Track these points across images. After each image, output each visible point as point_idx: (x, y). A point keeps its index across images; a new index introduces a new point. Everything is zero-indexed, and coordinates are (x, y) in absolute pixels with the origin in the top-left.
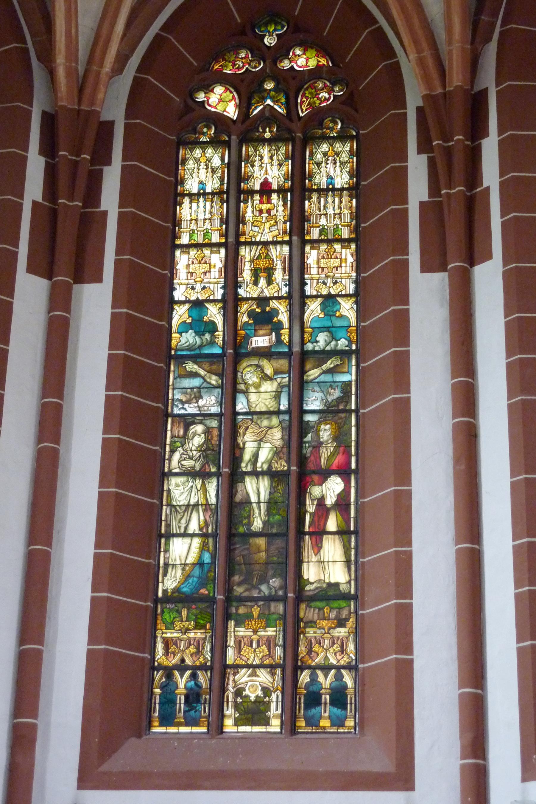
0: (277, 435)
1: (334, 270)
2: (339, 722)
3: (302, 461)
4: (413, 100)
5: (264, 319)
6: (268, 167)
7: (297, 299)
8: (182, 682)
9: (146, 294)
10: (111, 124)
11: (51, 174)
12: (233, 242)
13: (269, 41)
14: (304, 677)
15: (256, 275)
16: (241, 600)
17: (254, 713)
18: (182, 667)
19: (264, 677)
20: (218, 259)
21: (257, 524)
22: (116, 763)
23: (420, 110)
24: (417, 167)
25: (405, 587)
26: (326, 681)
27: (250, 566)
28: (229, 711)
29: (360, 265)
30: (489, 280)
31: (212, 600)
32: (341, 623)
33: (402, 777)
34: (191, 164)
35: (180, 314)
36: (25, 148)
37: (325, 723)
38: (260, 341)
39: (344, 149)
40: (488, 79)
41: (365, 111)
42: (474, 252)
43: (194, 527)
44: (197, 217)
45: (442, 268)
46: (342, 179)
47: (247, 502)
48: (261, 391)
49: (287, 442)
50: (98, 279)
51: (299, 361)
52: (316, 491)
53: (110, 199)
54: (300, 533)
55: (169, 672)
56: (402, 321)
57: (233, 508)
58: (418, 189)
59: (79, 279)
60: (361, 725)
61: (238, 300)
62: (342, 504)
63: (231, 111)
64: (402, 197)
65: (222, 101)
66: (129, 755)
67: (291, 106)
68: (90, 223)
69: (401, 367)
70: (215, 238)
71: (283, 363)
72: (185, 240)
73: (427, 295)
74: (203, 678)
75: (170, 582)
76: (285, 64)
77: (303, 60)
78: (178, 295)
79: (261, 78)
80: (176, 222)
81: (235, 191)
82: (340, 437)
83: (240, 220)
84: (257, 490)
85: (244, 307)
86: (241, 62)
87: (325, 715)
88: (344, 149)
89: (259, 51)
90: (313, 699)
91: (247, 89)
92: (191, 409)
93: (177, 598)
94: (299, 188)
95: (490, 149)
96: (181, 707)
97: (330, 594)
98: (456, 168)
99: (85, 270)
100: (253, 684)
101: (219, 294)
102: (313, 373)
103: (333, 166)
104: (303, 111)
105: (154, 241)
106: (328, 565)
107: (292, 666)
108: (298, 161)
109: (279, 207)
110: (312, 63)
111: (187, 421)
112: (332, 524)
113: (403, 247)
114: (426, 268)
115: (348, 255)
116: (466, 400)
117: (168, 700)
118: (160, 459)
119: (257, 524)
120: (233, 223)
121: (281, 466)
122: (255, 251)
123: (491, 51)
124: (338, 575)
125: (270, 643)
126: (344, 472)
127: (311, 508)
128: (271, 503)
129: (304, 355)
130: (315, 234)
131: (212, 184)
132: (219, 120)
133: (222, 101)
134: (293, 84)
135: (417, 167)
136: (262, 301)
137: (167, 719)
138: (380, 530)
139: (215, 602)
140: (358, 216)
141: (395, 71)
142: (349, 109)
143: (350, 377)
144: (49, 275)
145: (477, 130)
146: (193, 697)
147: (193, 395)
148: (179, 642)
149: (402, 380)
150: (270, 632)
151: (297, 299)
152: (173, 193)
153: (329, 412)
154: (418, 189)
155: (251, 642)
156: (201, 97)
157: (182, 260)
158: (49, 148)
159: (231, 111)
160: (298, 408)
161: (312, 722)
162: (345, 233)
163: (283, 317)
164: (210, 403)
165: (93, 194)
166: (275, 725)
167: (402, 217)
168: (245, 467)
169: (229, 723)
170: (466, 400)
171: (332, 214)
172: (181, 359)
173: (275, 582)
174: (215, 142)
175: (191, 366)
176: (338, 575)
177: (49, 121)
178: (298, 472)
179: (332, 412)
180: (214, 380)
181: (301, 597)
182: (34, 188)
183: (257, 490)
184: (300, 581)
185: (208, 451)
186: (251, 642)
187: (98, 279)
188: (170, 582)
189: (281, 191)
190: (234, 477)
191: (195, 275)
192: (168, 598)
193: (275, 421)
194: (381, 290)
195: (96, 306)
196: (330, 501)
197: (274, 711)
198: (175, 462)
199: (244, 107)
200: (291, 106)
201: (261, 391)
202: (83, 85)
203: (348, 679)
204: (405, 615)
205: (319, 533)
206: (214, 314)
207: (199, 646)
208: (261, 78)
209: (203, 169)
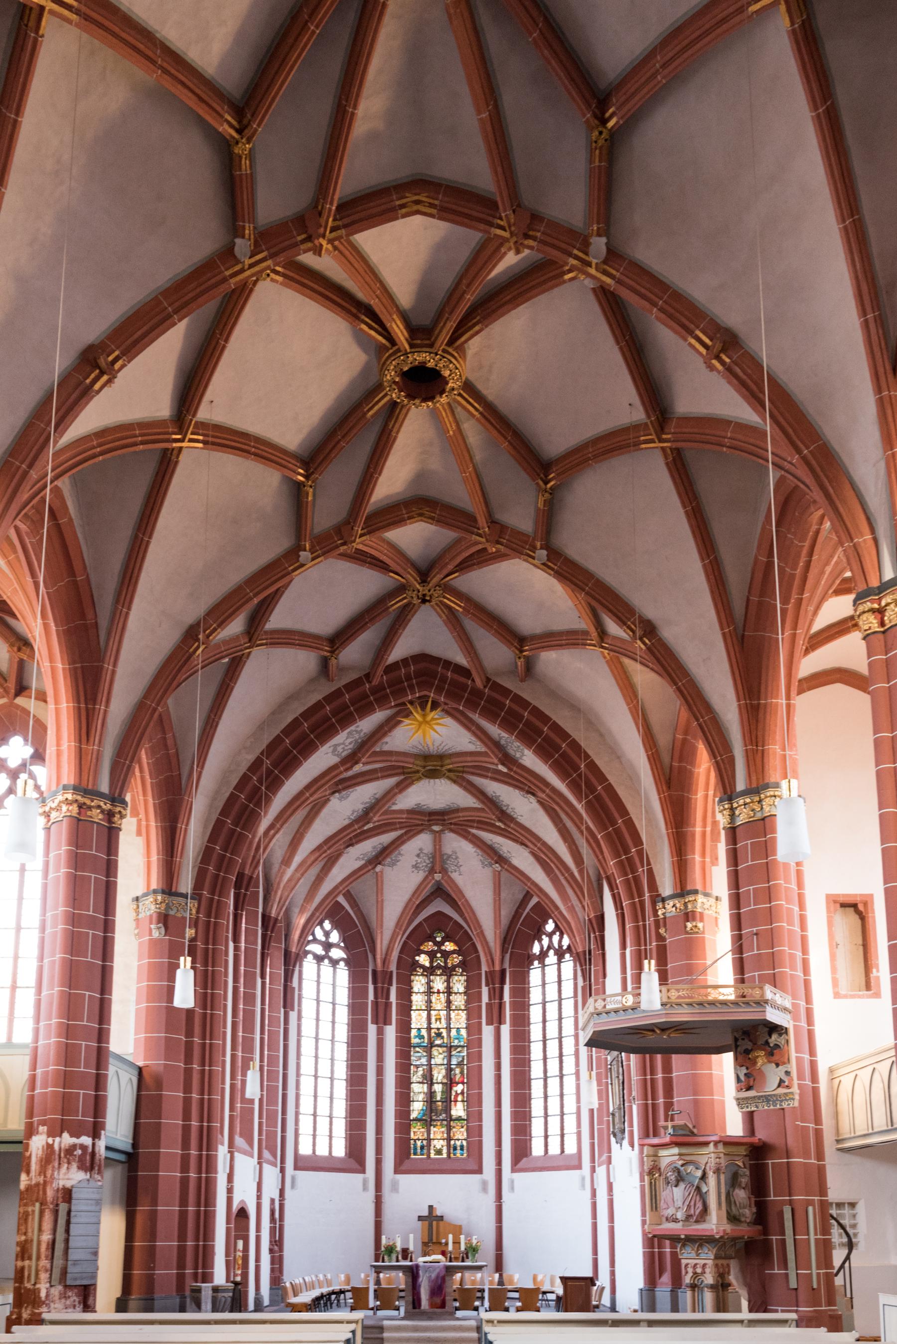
0: (443, 1072)
1: (460, 1019)
2: (462, 1155)
3: (451, 1080)
4: (484, 968)
5: (439, 1035)
6: (439, 983)
7: (449, 1029)
8: (419, 1143)
9: (405, 1027)
10: (391, 972)
11: (376, 989)
12: (429, 1009)
13: (438, 939)
14: (452, 1142)
15: (436, 1020)
16: (435, 1120)
17: (439, 1152)
18: (419, 1139)
19: (441, 1142)
21: (439, 1098)
22: (403, 1168)
23: (486, 972)
24: (485, 991)
25: (480, 1120)
26: (458, 1143)
27: (438, 1110)
28: (432, 1152)
29: (468, 1019)
30: (506, 1029)
31: (426, 1120)
32: (462, 1127)
33: (479, 1171)
34: (415, 982)
35: (414, 1033)
36: (367, 983)
37: (458, 1155)
38: (438, 1042)
39: (463, 978)
40: (506, 965)
41: (469, 965)
42: (501, 1021)
43: (421, 1099)
44: (418, 1000)
45: (492, 1024)
46: (462, 990)
47: (435, 1092)
48: (439, 1057)
49: (447, 1074)
50: (390, 1024)
51: (450, 1048)
52: (455, 1089)
53: (393, 998)
54: (451, 1101)
55: (415, 1140)
56: (480, 1040)
57: (431, 1094)
59: (385, 1024)
60: (468, 1155)
61: (431, 1029)
62: (462, 1093)
63: (427, 964)
64: (480, 1000)
65: (423, 960)
66: (406, 1165)
67: (446, 963)
68: (388, 1005)
69: (480, 1054)
70: (424, 1008)
71: (445, 1049)
72: (414, 1008)
73: (488, 1032)
74: (425, 1142)
76: (443, 948)
78: (412, 1026)
79: (437, 952)
80: (411, 1002)
81: (429, 991)
82: (462, 1073)
83: (431, 1002)
84: (438, 1088)
85: (433, 1031)
86: (429, 946)
87: (458, 1152)
88: (463, 978)
89: (436, 943)
90: (455, 1149)
91: (432, 955)
92: (418, 1063)
93: (416, 1119)
94: (449, 991)
96: (419, 1151)
97: (459, 1119)
99: (387, 1022)
100: (439, 1144)
101: (425, 1026)
102: (454, 1053)
103: (459, 984)
104: (450, 965)
105: (406, 1008)
106: (458, 1110)
107: (449, 1139)
108: (448, 981)
109: (443, 997)
110: (452, 948)
111: (417, 1067)
112: (460, 1098)
113: (480, 1017)
114: (487, 1024)
116: (498, 1066)
117: (415, 1149)
118: (409, 1078)
119: (439, 1098)
120: (429, 1002)
121: (445, 1081)
122: (436, 1012)
123: (508, 956)
125: (443, 1132)
126: (463, 1083)
127: (454, 1093)
128: (442, 1092)
129: (451, 1047)
130: (454, 1007)
131: (422, 989)
132: (422, 967)
133: (423, 960)
134: (446, 955)
135: (485, 991)
136: (438, 1029)
137: (415, 1154)
138: (474, 1101)
139: (427, 1121)
140: (467, 1002)
141: (478, 957)
142: (463, 965)
143: (465, 1054)
144: (377, 1024)
145: (503, 982)
146: (422, 1148)
147: (418, 1058)
148: (417, 1132)
149: (480, 1058)
150: (443, 1129)
151: (449, 1029)
156: (417, 958)
158: (375, 982)
159: (427, 964)
160: (449, 1064)
161: (454, 1154)
162: (463, 1007)
163: (445, 1034)
164: (424, 1061)
165: (388, 997)
166: (445, 1156)
167: (480, 1007)
168: (434, 1081)
169: (432, 1156)
171: (459, 1001)
172: (415, 1047)
173: (444, 1115)
174: (422, 975)
175: (417, 1049)
177: (374, 972)
178: (450, 1083)
179: (460, 1064)
180: (425, 1054)
181: (451, 1120)
182: (371, 997)
183: (438, 1088)
184: (451, 1116)
185: (424, 1076)
186: (438, 1132)
187: (390, 1024)
188: (414, 1115)
189: (443, 993)
190: (431, 1084)
191: (418, 1020)
192: (414, 1120)
193: (443, 1067)
194: (474, 1029)
195: (391, 1032)
196: (459, 1092)
197: (445, 1151)
198: (414, 1079)
199: (431, 962)
200: (446, 963)
201: (439, 1057)
202: (385, 961)
203: (465, 1143)
204: (480, 1127)
205: (456, 1101)
206: (424, 1032)
207: (423, 1133)
208: (437, 952)
209: (419, 983)
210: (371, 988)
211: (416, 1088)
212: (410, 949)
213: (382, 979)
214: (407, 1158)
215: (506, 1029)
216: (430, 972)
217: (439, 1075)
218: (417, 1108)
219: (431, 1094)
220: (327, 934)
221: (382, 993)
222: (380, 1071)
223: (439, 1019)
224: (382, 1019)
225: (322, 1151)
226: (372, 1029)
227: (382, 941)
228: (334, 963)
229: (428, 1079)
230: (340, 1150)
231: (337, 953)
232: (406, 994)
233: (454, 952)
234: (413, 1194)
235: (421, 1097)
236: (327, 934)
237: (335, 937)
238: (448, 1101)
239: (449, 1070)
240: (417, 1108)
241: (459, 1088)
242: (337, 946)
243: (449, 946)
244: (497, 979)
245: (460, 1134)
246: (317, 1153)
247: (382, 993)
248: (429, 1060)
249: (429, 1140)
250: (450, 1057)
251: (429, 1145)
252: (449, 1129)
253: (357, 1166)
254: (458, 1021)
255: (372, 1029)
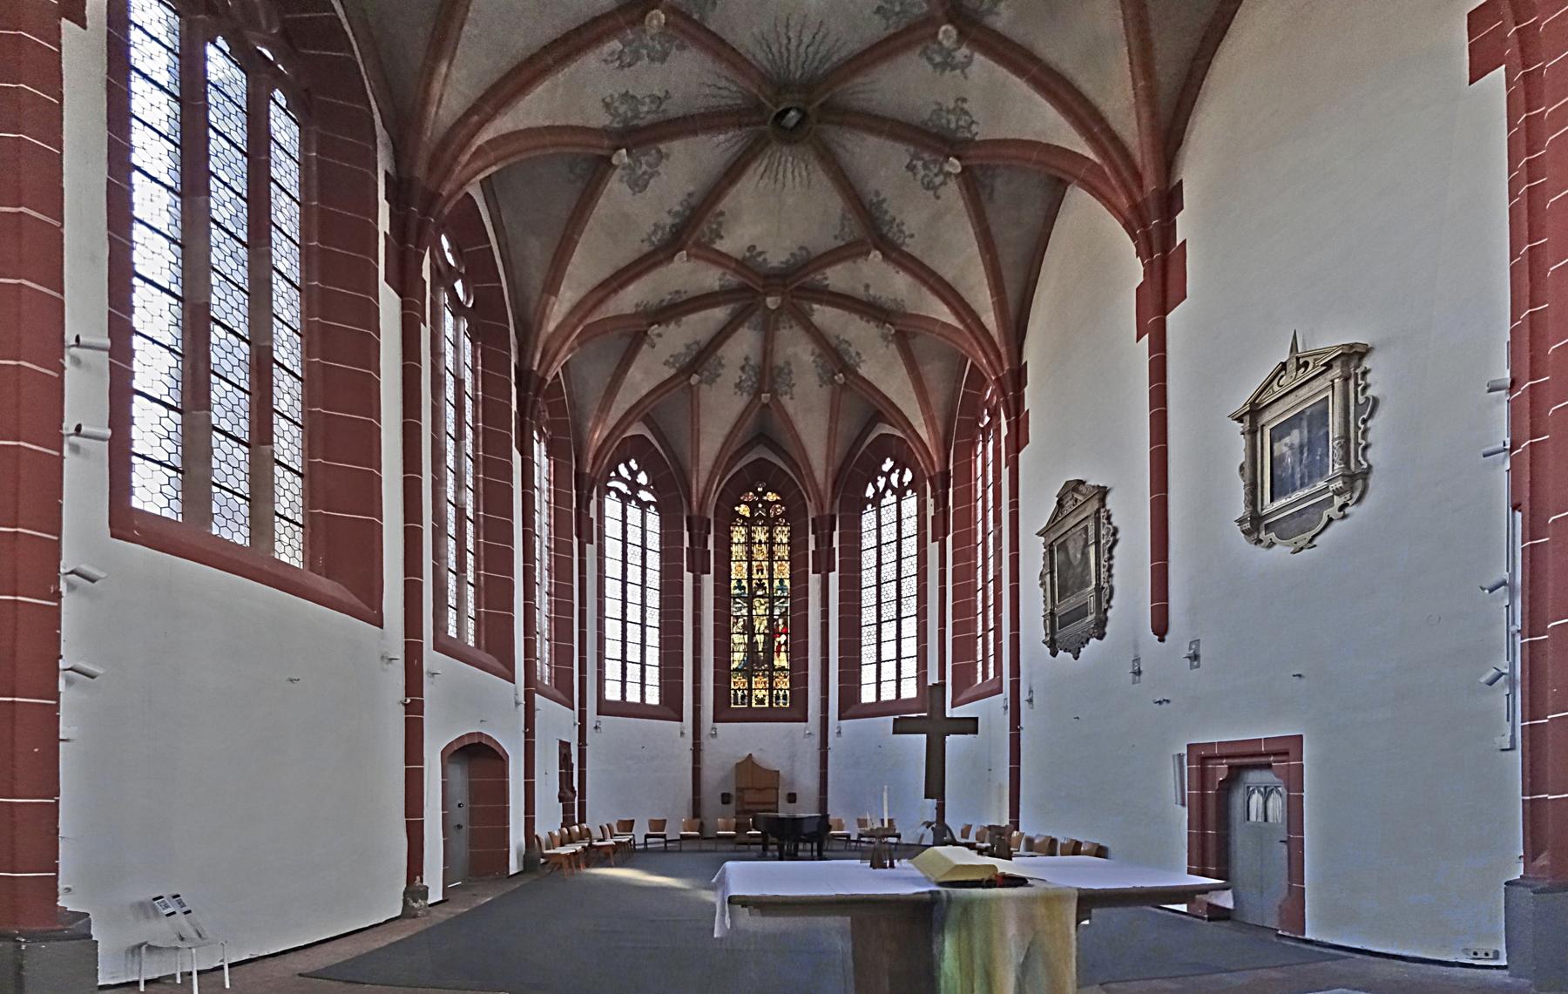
1: (783, 571)
5: (761, 586)
6: (761, 535)
7: (771, 580)
9: (723, 577)
12: (750, 560)
17: (761, 701)
20: (745, 565)
24: (811, 538)
27: (758, 662)
29: (791, 569)
30: (834, 577)
35: (734, 583)
44: (737, 551)
46: (785, 540)
48: (760, 609)
51: (772, 599)
53: (711, 546)
58: (812, 547)
65: (743, 510)
67: (768, 513)
73: (814, 580)
75: (734, 666)
77: (771, 497)
81: (750, 542)
82: (785, 623)
84: (760, 638)
89: (756, 493)
91: (752, 506)
93: (736, 670)
94: (771, 542)
95: (836, 535)
97: (782, 669)
98: (824, 541)
103: (782, 535)
105: (725, 558)
106: (782, 660)
107: (771, 689)
108: (770, 532)
115: (787, 565)
116: (825, 614)
120: (750, 553)
124: (785, 664)
132: (743, 517)
133: (743, 510)
135: (811, 538)
138: (798, 652)
139: (748, 671)
147: (739, 610)
148: (738, 682)
151: (771, 580)
152: (730, 543)
153: (781, 615)
154: (812, 547)
155: (759, 682)
157: (733, 565)
164: (744, 612)
170: (825, 614)
171: (782, 552)
176: (785, 664)
178: (772, 633)
183: (760, 638)
186: (759, 682)
188: (734, 666)
190: (752, 635)
191: (738, 571)
194: (799, 579)
195: (708, 581)
198: (734, 630)
201: (760, 609)
202: (702, 504)
205: (779, 651)
206: (745, 583)
209: (738, 534)
210: (686, 534)
211: (736, 638)
212: (728, 500)
213: (699, 529)
214: (723, 713)
215: (834, 577)
216: (749, 523)
217: (761, 625)
218: (738, 658)
219: (751, 646)
220: (634, 474)
221: (698, 541)
222: (697, 619)
223: (760, 570)
224: (699, 569)
225: (633, 696)
226: (688, 577)
227: (698, 484)
228: (643, 506)
229: (749, 629)
230: (653, 698)
231: (645, 496)
232: (725, 544)
233: (776, 502)
234: (733, 742)
235: (742, 648)
236: (634, 474)
237: (642, 478)
238: (770, 651)
239: (771, 620)
240: (738, 658)
241: (783, 638)
242: (646, 488)
243: (771, 497)
244: (824, 528)
245: (783, 684)
246: (629, 699)
247: (698, 541)
248: (750, 612)
249: (750, 689)
250: (772, 608)
251: (750, 695)
252: (771, 679)
253: (672, 714)
254: (781, 572)
255: (688, 577)
